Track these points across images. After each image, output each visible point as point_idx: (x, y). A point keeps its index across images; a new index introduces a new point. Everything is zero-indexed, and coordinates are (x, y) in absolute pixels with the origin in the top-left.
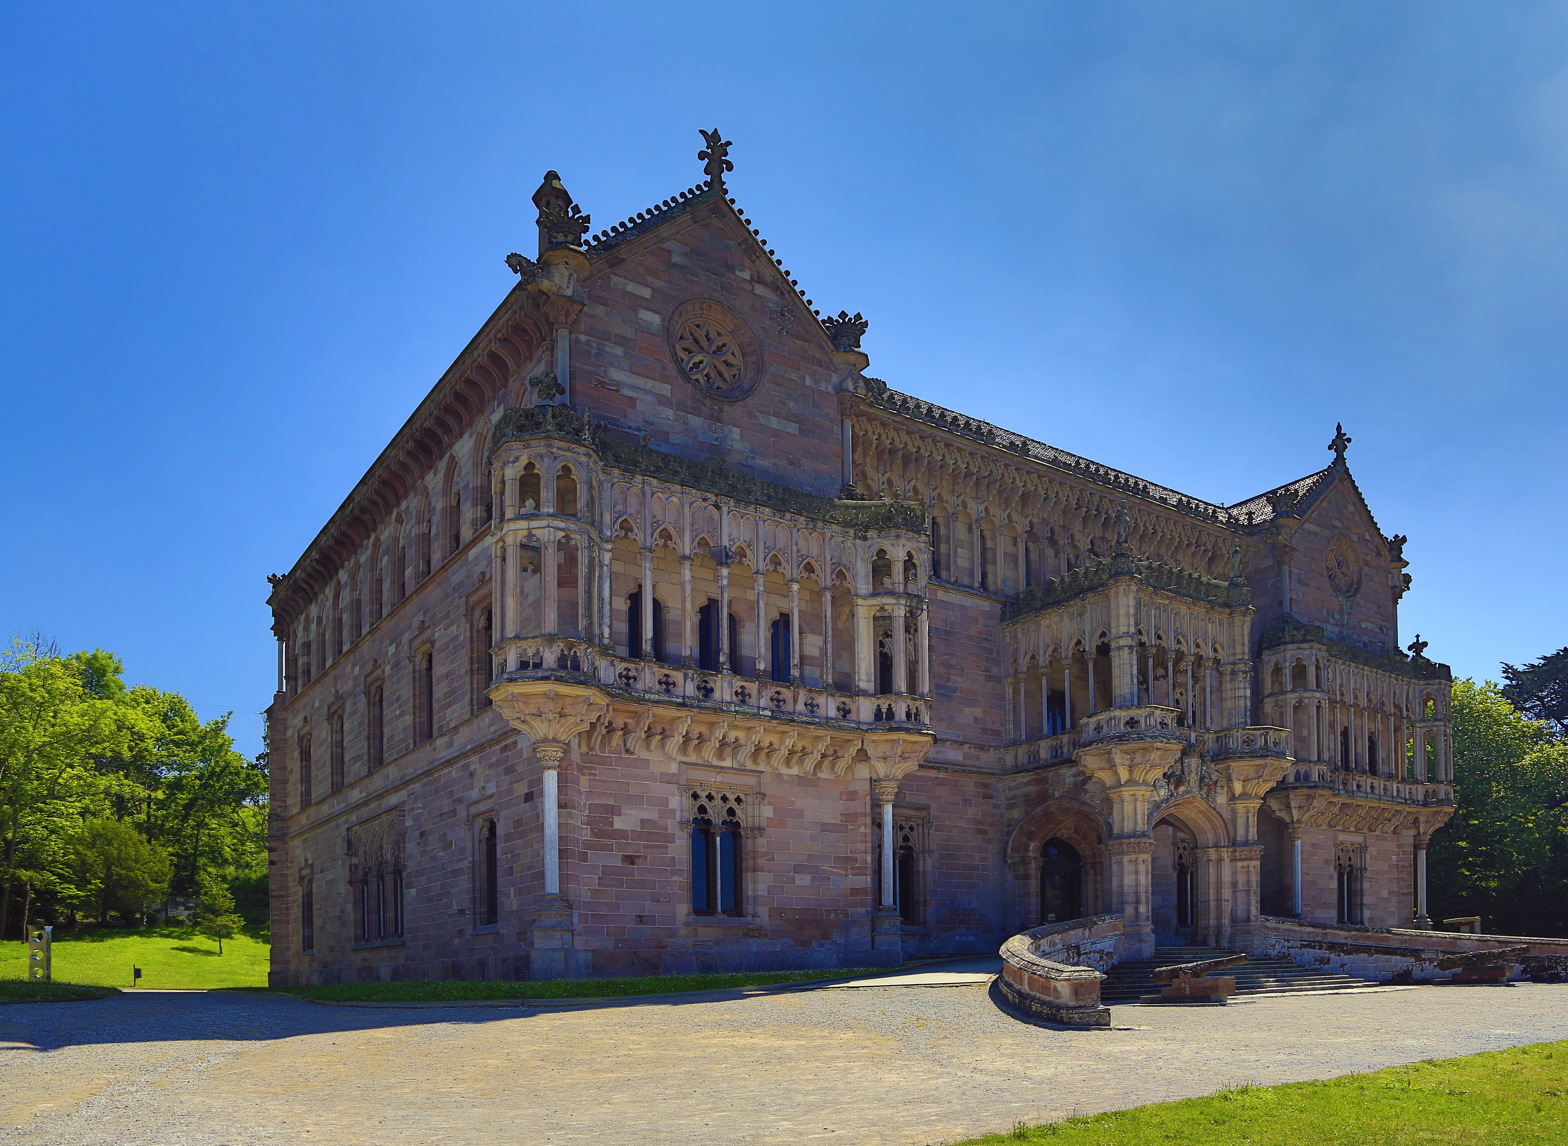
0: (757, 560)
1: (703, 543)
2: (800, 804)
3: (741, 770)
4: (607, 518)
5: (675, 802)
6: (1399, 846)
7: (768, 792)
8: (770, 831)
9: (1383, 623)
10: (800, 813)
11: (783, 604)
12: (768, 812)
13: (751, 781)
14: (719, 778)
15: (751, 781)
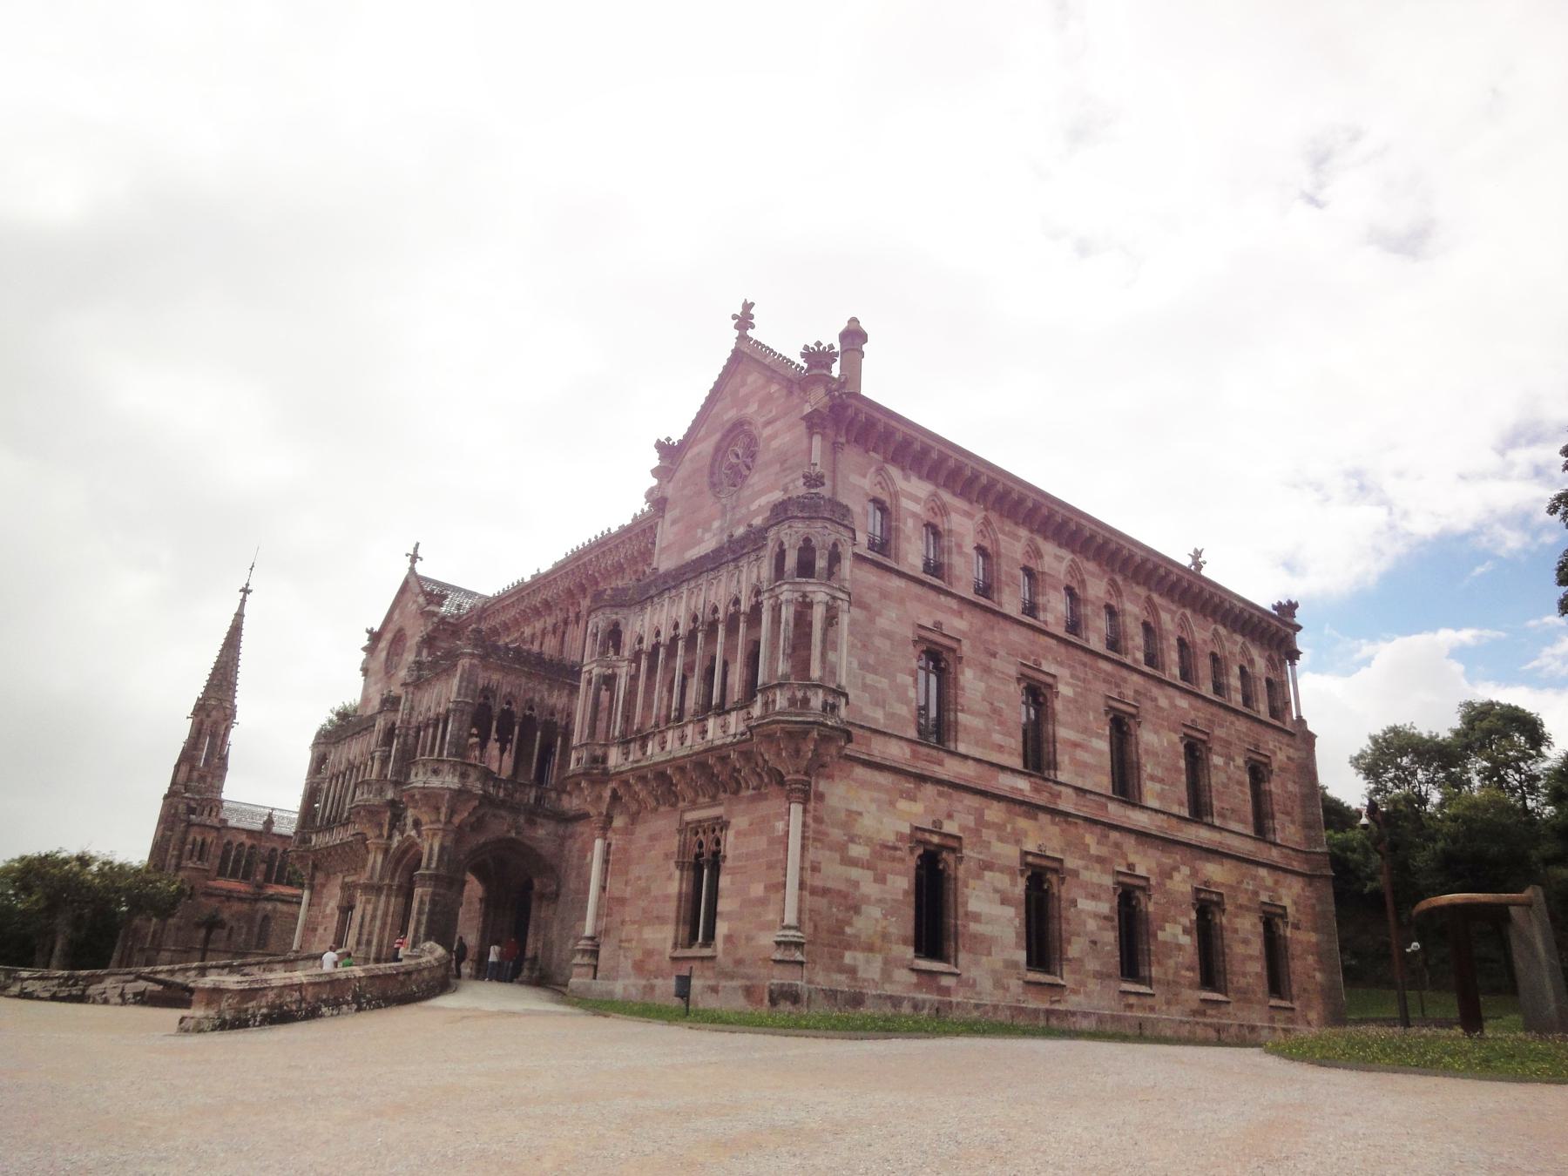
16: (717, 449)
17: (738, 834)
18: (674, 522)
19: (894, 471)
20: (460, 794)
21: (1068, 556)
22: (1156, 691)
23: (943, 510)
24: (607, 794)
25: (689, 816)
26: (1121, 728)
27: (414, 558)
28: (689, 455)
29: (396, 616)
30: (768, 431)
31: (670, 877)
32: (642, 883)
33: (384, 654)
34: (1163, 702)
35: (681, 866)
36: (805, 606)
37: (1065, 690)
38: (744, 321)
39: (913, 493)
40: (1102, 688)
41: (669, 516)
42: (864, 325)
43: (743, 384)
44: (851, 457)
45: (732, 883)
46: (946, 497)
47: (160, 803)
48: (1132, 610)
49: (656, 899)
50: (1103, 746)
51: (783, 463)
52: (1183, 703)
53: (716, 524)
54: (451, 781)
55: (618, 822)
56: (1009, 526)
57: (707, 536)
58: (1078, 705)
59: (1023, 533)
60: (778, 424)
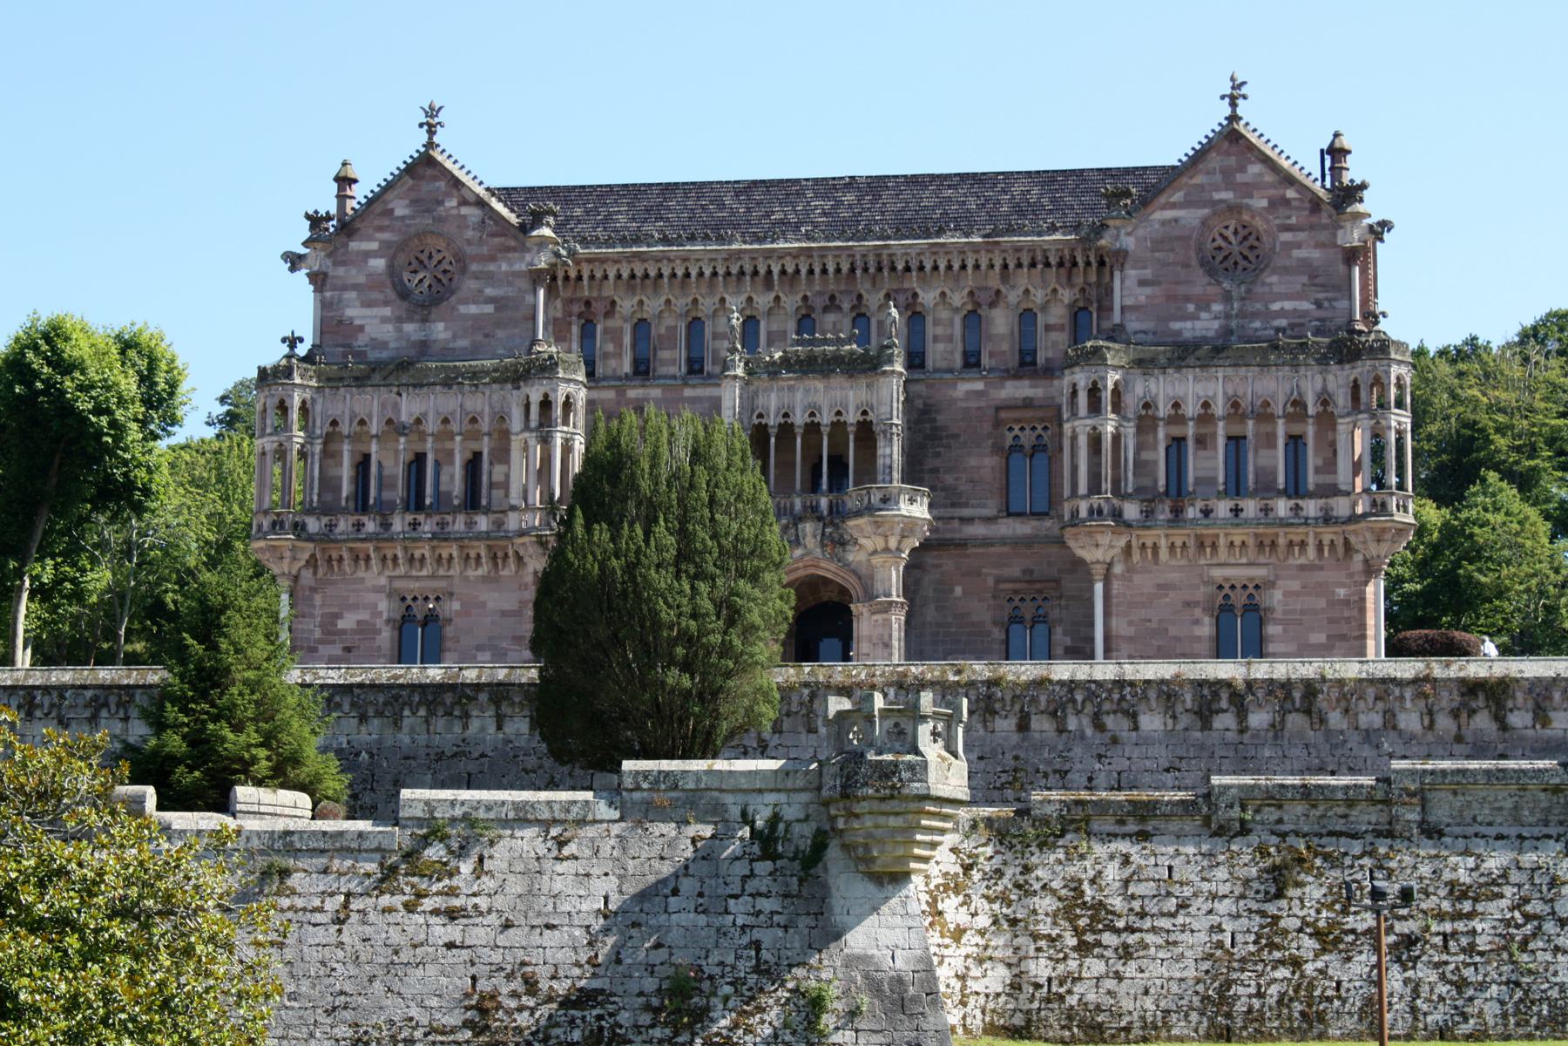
0: (431, 426)
1: (389, 422)
2: (483, 597)
3: (433, 577)
4: (318, 423)
5: (383, 605)
6: (1351, 575)
7: (456, 590)
8: (456, 621)
9: (1321, 296)
10: (483, 604)
11: (475, 446)
12: (456, 606)
13: (442, 584)
14: (417, 585)
15: (442, 584)
16: (1204, 222)
17: (1286, 594)
18: (1142, 283)
24: (1122, 542)
25: (1217, 573)
28: (1159, 215)
30: (1286, 237)
31: (1197, 622)
32: (1154, 625)
33: (379, 264)
35: (1208, 610)
41: (1132, 274)
42: (1345, 142)
43: (1242, 169)
45: (1285, 631)
49: (1178, 639)
51: (1312, 277)
53: (1217, 307)
55: (1118, 569)
57: (1203, 315)
60: (1302, 236)
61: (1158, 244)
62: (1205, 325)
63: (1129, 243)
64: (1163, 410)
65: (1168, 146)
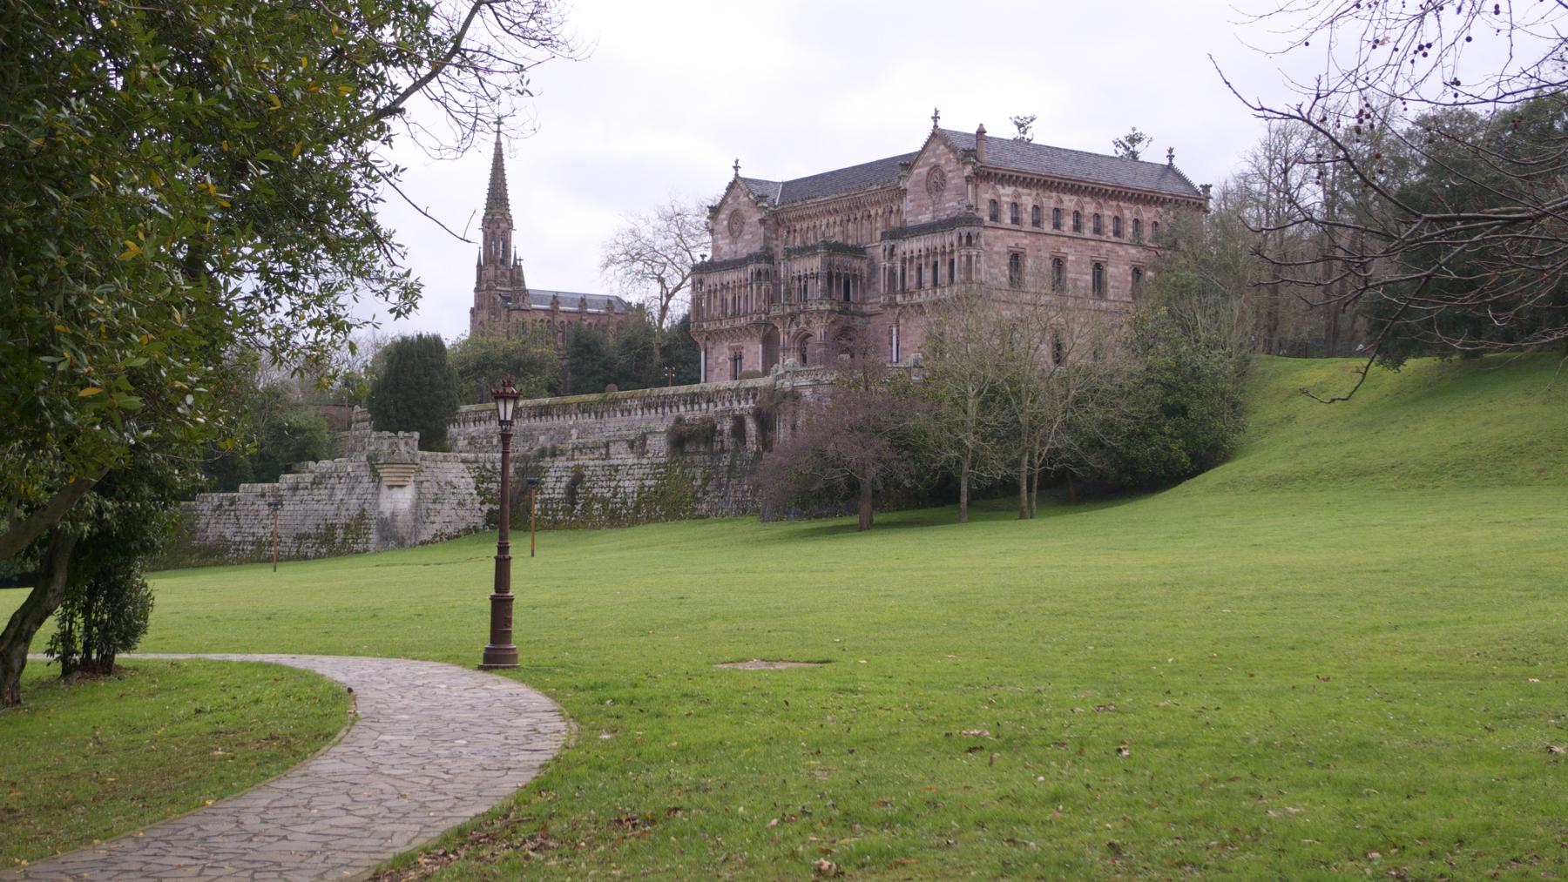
19: (999, 187)
20: (832, 311)
21: (1075, 198)
22: (1117, 248)
23: (1019, 196)
26: (1098, 268)
27: (736, 168)
29: (730, 200)
34: (1122, 253)
36: (969, 258)
37: (1070, 258)
38: (936, 118)
39: (1006, 193)
40: (1090, 253)
44: (982, 186)
46: (1020, 190)
47: (472, 295)
48: (1108, 213)
50: (1089, 278)
52: (1133, 251)
54: (828, 307)
55: (902, 321)
56: (1048, 193)
58: (1077, 262)
59: (1054, 194)
61: (916, 184)
62: (926, 218)
63: (908, 185)
64: (908, 256)
65: (913, 143)
